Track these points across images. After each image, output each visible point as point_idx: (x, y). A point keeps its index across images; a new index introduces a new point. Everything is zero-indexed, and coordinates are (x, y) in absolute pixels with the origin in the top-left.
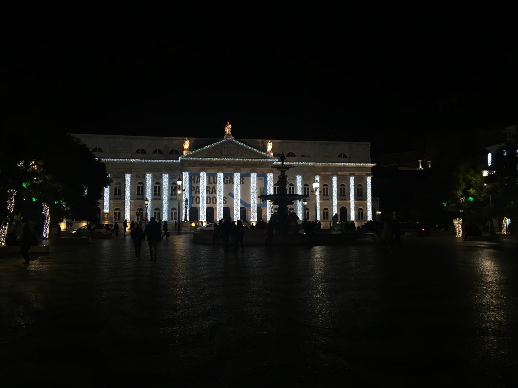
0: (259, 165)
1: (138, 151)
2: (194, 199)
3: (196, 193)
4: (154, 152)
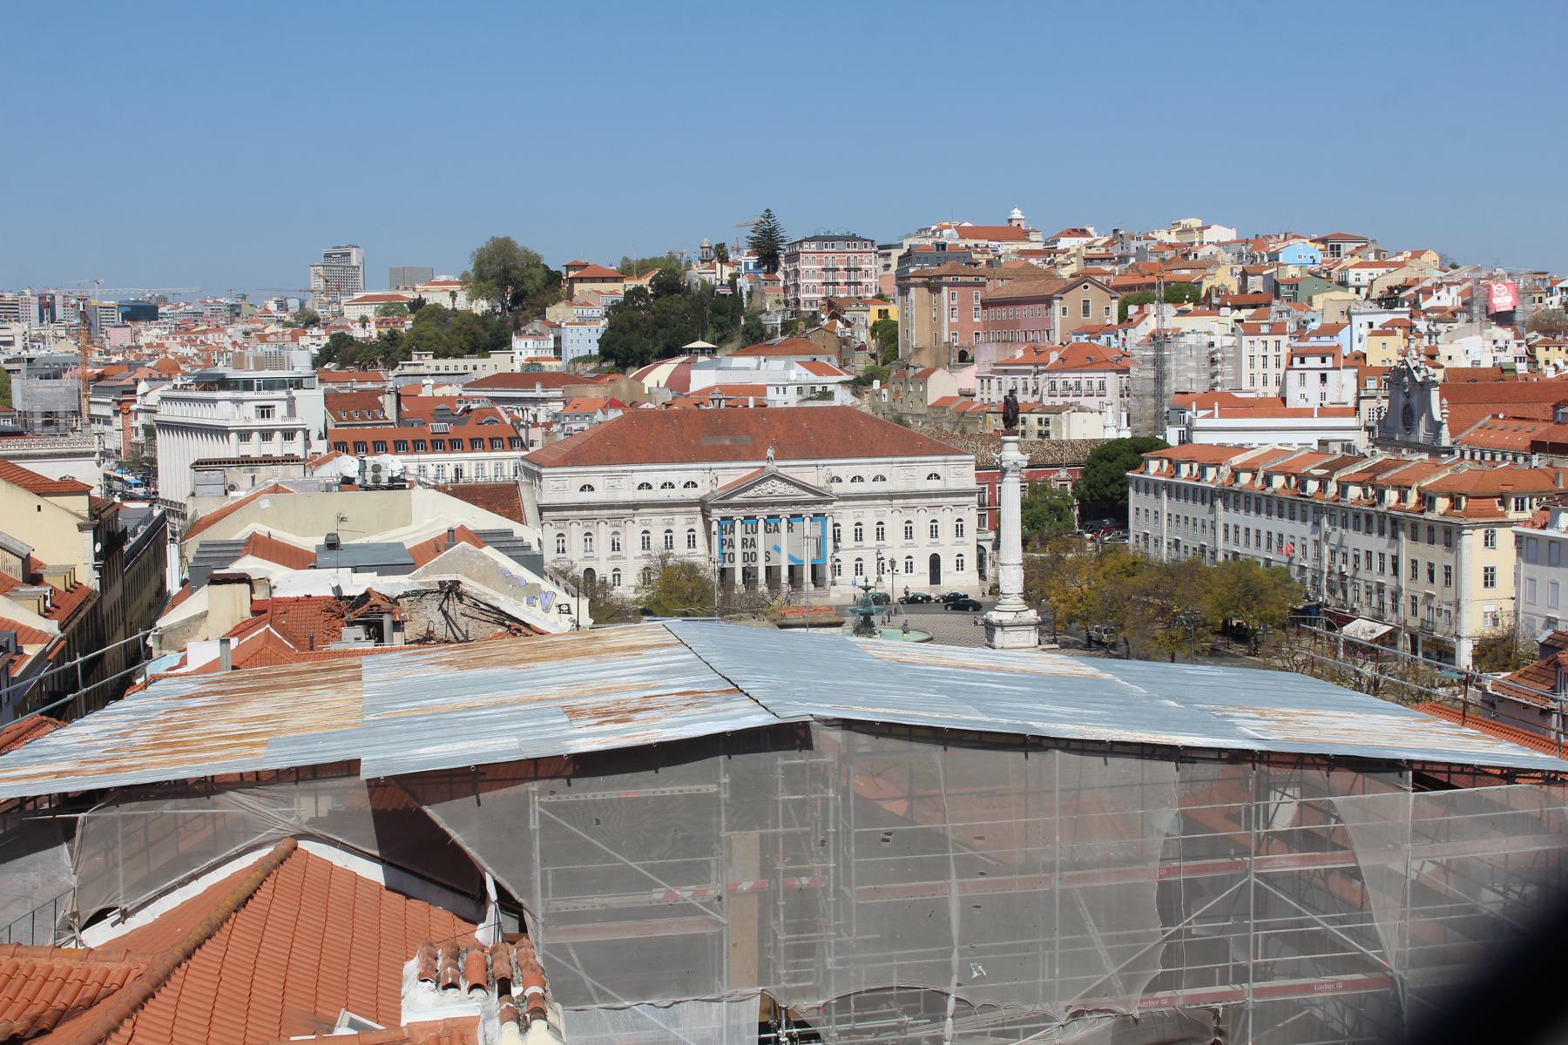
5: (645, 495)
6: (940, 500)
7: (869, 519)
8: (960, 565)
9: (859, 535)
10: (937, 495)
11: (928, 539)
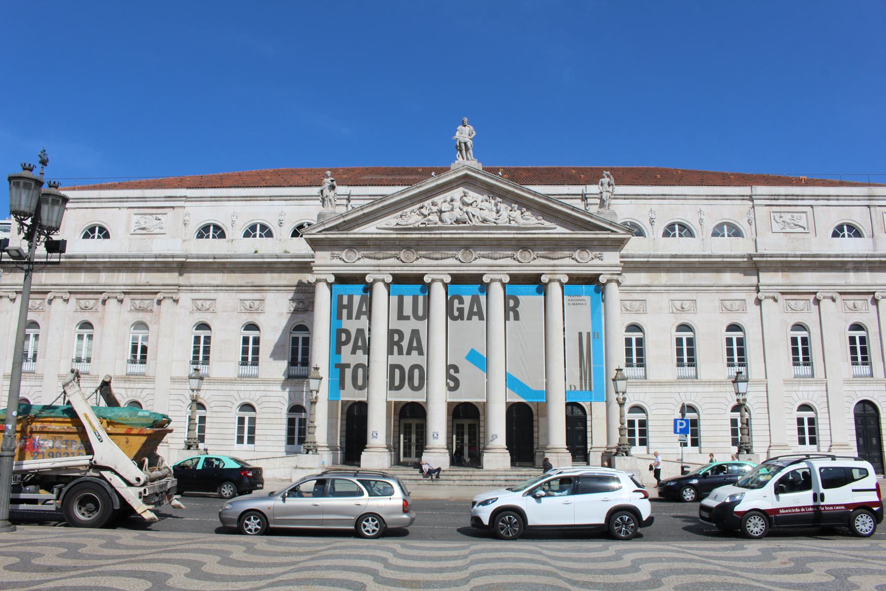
1: (203, 232)
2: (348, 373)
3: (354, 352)
4: (247, 235)
5: (211, 247)
6: (866, 279)
9: (687, 353)
10: (859, 266)
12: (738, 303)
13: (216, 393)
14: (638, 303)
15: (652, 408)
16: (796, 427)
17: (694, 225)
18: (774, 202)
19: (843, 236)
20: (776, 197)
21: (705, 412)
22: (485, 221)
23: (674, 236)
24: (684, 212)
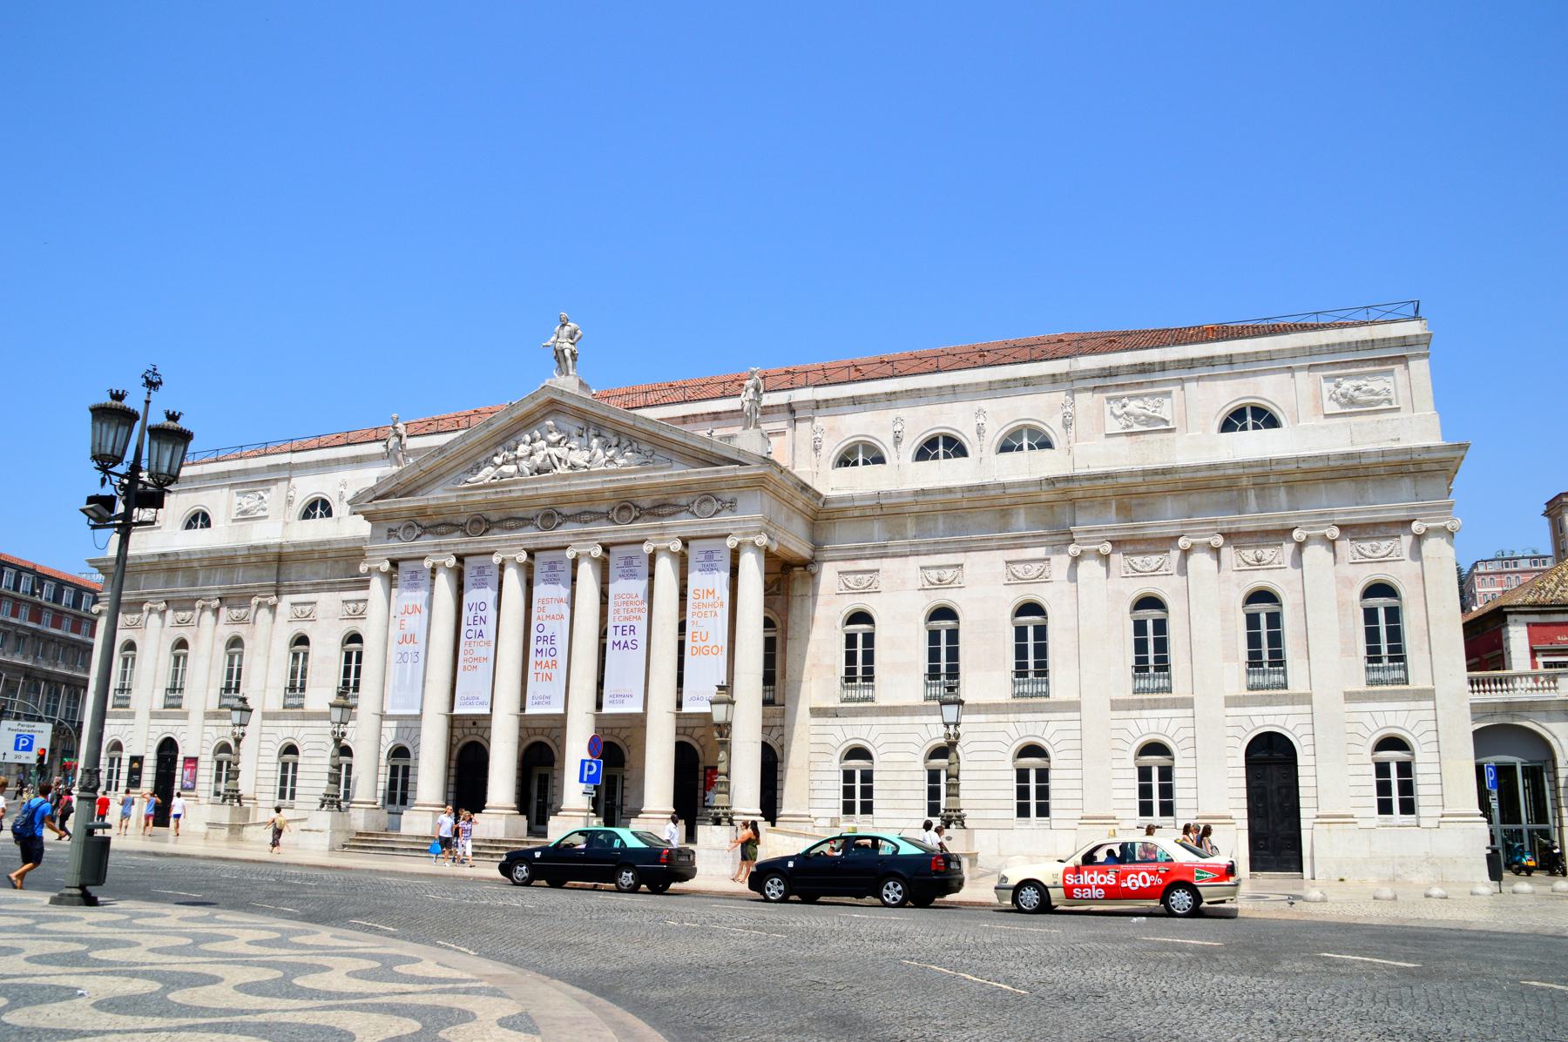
0: (687, 508)
1: (307, 514)
7: (985, 589)
8: (1396, 788)
9: (944, 660)
11: (1233, 672)
12: (1036, 566)
13: (309, 730)
14: (867, 577)
15: (880, 750)
16: (1136, 783)
17: (968, 437)
18: (1109, 382)
19: (1244, 428)
20: (1110, 373)
21: (969, 757)
22: (573, 466)
23: (936, 457)
24: (954, 418)
